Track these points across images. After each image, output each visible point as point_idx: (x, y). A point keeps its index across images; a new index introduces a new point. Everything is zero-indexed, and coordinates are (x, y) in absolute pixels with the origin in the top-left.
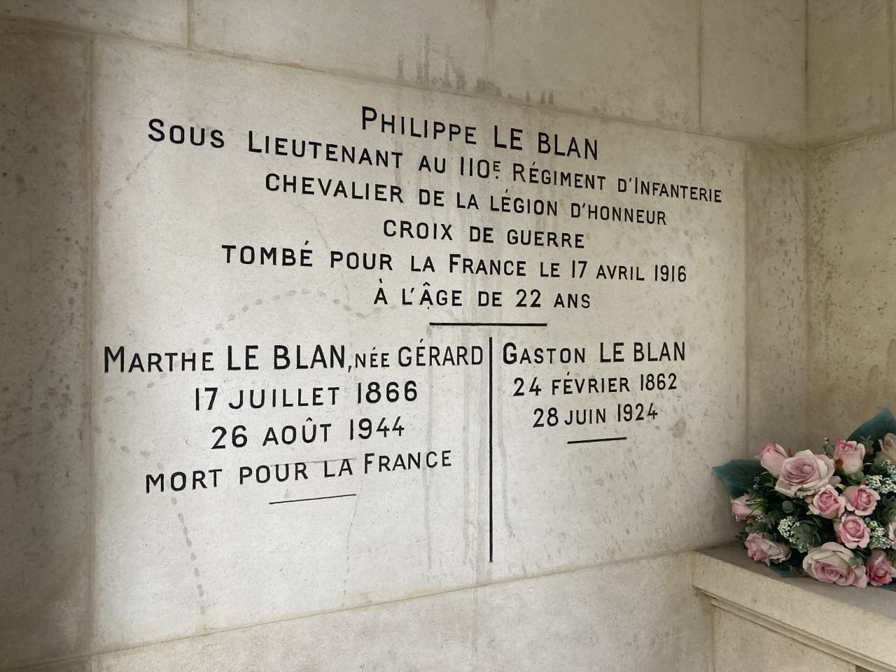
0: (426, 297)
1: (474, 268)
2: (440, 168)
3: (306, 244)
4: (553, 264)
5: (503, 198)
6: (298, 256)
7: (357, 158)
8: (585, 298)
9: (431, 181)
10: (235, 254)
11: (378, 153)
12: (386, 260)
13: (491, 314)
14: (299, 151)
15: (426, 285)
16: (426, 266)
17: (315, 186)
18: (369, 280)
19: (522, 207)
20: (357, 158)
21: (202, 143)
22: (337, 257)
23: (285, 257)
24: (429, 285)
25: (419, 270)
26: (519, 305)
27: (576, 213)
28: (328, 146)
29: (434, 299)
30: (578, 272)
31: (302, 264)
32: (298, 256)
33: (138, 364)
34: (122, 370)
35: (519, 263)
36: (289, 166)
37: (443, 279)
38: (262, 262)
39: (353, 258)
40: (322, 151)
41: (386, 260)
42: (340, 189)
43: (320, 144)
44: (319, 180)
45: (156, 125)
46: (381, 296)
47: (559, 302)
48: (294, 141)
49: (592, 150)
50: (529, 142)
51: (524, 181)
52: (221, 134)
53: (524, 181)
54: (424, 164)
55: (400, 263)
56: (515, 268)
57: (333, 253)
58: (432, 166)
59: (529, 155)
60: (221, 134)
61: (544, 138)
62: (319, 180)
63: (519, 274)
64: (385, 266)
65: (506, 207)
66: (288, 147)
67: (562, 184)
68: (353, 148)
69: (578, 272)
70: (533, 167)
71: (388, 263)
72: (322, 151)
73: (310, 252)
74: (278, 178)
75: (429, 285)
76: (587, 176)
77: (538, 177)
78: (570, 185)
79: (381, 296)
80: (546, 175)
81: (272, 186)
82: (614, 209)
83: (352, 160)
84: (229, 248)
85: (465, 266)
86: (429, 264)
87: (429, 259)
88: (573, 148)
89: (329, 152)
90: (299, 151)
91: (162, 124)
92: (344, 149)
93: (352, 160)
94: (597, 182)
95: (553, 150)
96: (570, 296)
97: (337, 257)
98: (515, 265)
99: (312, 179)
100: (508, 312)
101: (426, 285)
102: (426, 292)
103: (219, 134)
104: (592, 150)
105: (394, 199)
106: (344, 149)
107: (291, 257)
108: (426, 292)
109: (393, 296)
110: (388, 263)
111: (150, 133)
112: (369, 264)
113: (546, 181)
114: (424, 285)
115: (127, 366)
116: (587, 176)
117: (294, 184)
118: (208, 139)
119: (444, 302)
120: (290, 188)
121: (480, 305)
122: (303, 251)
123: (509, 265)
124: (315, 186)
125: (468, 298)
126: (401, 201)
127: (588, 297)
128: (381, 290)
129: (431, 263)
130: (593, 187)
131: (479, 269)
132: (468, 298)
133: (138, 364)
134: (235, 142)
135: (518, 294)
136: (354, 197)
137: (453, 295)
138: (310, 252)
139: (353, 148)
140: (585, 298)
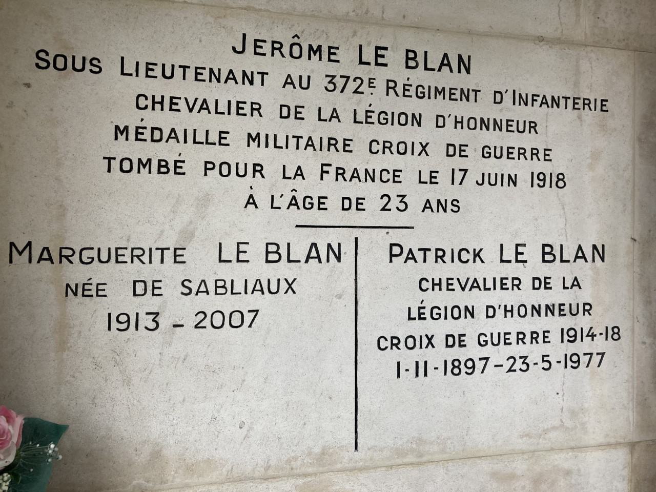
0: (293, 202)
1: (348, 175)
2: (305, 85)
3: (179, 155)
4: (431, 172)
5: (367, 112)
6: (171, 166)
7: (223, 79)
8: (455, 203)
9: (293, 97)
10: (115, 165)
11: (244, 73)
12: (258, 169)
13: (354, 217)
14: (168, 74)
15: (294, 191)
16: (296, 174)
17: (182, 105)
18: (240, 187)
19: (387, 119)
20: (223, 79)
21: (83, 69)
22: (210, 166)
23: (160, 166)
24: (296, 191)
25: (290, 178)
26: (383, 209)
27: (441, 124)
28: (196, 68)
29: (301, 204)
30: (457, 181)
31: (176, 173)
32: (171, 166)
33: (47, 257)
34: (30, 261)
35: (395, 171)
36: (158, 88)
37: (311, 186)
38: (139, 172)
39: (225, 167)
40: (190, 73)
41: (258, 169)
42: (204, 106)
43: (189, 67)
44: (186, 99)
45: (42, 55)
46: (251, 201)
47: (427, 206)
48: (164, 65)
49: (465, 65)
50: (394, 58)
51: (397, 95)
52: (99, 62)
53: (397, 95)
54: (289, 81)
55: (272, 170)
56: (391, 176)
57: (206, 163)
58: (297, 84)
59: (396, 69)
60: (99, 62)
61: (411, 55)
62: (186, 99)
63: (394, 181)
64: (258, 174)
65: (369, 120)
66: (158, 71)
67: (436, 98)
68: (219, 70)
69: (457, 181)
70: (407, 83)
71: (260, 171)
72: (190, 73)
73: (183, 162)
74: (146, 98)
75: (296, 191)
76: (462, 90)
77: (412, 92)
78: (444, 98)
79: (251, 201)
80: (420, 89)
81: (142, 105)
82: (482, 120)
83: (218, 80)
84: (110, 159)
85: (337, 174)
86: (299, 172)
87: (299, 168)
88: (445, 62)
89: (197, 74)
90: (168, 74)
91: (47, 54)
92: (211, 70)
93: (218, 80)
94: (472, 94)
95: (421, 65)
96: (439, 201)
97: (210, 166)
98: (391, 173)
99: (180, 98)
100: (333, 214)
101: (294, 191)
102: (294, 198)
103: (97, 61)
104: (465, 65)
105: (254, 114)
106: (211, 70)
107: (166, 166)
108: (294, 198)
109: (263, 200)
110: (260, 171)
111: (36, 62)
112: (242, 172)
113: (420, 95)
114: (292, 191)
115: (35, 257)
116: (462, 90)
117: (162, 103)
118: (88, 66)
119: (310, 206)
120: (158, 106)
121: (343, 209)
122: (176, 162)
123: (385, 173)
124: (182, 105)
125: (334, 203)
126: (261, 116)
127: (458, 202)
128: (251, 196)
129: (301, 171)
130: (468, 100)
131: (353, 177)
132: (334, 203)
133: (47, 257)
134: (111, 68)
135: (382, 198)
136: (217, 113)
137: (319, 200)
138: (183, 162)
139: (219, 70)
140: (455, 203)
